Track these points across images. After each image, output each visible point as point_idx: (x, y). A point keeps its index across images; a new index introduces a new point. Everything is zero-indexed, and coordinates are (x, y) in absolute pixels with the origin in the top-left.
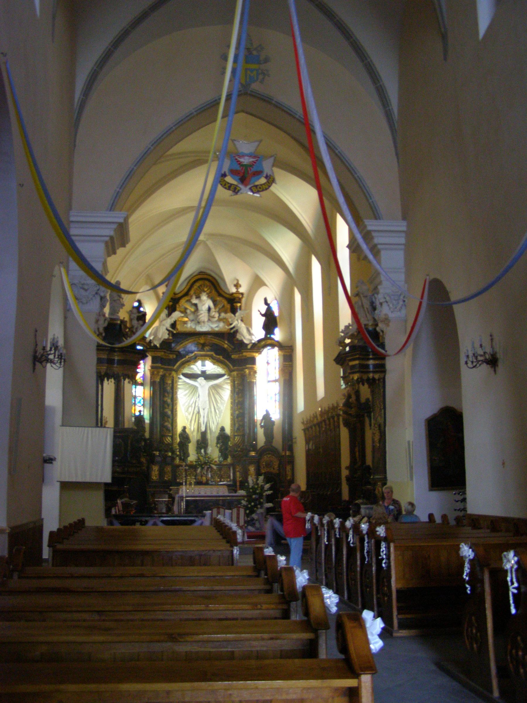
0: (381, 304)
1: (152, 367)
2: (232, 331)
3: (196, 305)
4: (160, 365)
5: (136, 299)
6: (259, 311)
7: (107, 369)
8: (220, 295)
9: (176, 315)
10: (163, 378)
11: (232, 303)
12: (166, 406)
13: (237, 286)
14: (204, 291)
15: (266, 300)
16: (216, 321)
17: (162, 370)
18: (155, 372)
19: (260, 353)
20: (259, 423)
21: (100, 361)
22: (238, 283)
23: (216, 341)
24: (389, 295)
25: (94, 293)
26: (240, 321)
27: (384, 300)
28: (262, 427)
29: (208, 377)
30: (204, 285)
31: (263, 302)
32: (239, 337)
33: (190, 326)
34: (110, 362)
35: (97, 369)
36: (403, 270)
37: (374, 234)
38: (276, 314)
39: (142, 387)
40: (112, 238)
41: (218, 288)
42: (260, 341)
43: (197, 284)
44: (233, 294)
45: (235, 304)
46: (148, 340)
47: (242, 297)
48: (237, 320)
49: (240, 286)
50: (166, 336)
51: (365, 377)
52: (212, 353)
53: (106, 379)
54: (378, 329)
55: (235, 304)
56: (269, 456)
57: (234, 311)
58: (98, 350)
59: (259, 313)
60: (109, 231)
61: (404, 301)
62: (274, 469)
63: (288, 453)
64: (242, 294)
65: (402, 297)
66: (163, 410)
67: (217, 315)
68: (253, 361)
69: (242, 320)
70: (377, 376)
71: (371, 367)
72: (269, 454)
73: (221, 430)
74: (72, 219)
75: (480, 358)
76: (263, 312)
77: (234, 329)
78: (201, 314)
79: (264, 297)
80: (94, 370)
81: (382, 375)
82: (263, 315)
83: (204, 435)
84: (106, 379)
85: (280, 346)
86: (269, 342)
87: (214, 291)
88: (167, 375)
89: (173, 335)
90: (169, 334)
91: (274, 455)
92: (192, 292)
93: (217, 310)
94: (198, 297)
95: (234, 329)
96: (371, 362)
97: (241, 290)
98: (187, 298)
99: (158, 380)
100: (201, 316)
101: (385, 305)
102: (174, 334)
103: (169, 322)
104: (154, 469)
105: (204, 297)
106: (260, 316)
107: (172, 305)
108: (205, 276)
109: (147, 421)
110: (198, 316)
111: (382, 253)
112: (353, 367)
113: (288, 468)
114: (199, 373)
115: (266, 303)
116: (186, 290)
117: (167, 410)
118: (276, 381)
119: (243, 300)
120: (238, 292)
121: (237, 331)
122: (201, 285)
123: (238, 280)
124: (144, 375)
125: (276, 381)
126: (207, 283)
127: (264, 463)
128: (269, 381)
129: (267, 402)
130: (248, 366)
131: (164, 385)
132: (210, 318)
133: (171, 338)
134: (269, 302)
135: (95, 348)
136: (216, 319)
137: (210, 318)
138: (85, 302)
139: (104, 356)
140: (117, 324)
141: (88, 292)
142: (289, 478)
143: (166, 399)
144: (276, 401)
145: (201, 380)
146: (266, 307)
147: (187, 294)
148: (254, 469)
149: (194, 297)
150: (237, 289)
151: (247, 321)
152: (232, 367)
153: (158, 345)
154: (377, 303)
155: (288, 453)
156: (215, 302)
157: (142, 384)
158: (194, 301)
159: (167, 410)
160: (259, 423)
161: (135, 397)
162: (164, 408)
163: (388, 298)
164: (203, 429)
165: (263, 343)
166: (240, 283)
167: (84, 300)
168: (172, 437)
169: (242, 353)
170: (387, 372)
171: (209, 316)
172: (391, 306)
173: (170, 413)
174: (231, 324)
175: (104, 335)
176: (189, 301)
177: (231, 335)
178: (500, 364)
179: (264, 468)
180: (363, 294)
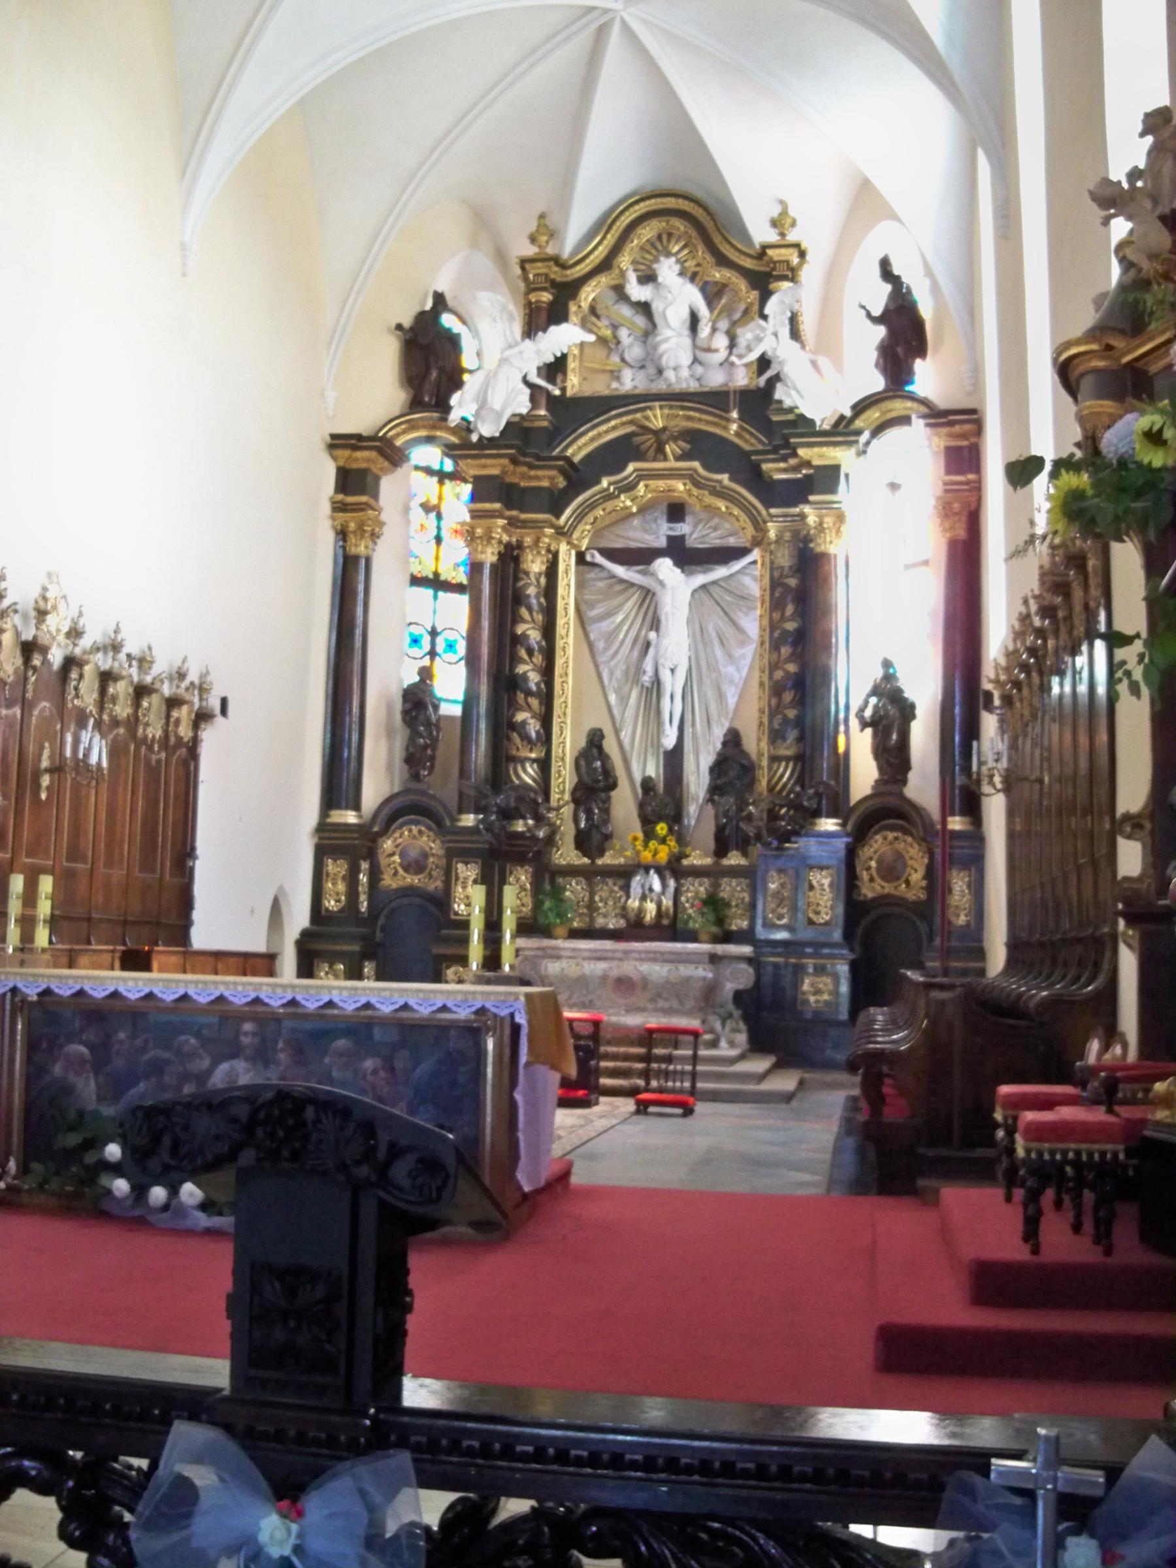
1: (475, 515)
2: (762, 381)
3: (645, 308)
4: (497, 506)
6: (863, 307)
8: (722, 261)
9: (564, 337)
10: (510, 558)
12: (523, 653)
14: (668, 254)
15: (885, 265)
17: (501, 522)
18: (479, 531)
22: (784, 213)
23: (704, 422)
28: (864, 725)
29: (686, 556)
30: (670, 235)
31: (877, 270)
32: (779, 393)
33: (630, 382)
38: (926, 310)
41: (717, 240)
43: (647, 232)
44: (765, 247)
47: (801, 264)
49: (794, 224)
50: (522, 404)
52: (696, 464)
56: (891, 835)
59: (864, 312)
62: (907, 882)
63: (956, 823)
66: (512, 667)
67: (721, 342)
72: (893, 828)
73: (724, 744)
76: (877, 311)
78: (666, 340)
79: (881, 256)
82: (876, 320)
83: (674, 759)
85: (937, 416)
86: (898, 407)
87: (701, 250)
88: (528, 541)
89: (555, 404)
90: (533, 399)
91: (906, 832)
92: (624, 261)
93: (724, 325)
94: (648, 278)
97: (792, 237)
98: (604, 279)
99: (489, 556)
100: (662, 348)
102: (555, 397)
104: (461, 876)
105: (667, 270)
106: (868, 322)
107: (551, 304)
108: (670, 203)
109: (456, 710)
110: (655, 348)
113: (959, 883)
114: (662, 543)
116: (601, 252)
117: (521, 669)
119: (805, 274)
122: (660, 237)
123: (781, 202)
126: (679, 224)
127: (873, 864)
129: (887, 629)
130: (812, 498)
131: (517, 579)
132: (702, 356)
133: (542, 412)
136: (723, 354)
137: (702, 356)
142: (962, 920)
143: (520, 629)
145: (665, 567)
146: (888, 288)
147: (605, 266)
148: (831, 885)
149: (632, 277)
150: (783, 235)
152: (764, 512)
155: (956, 823)
158: (637, 292)
159: (521, 669)
162: (515, 660)
164: (670, 741)
165: (874, 415)
166: (792, 212)
168: (544, 765)
169: (795, 454)
171: (695, 346)
173: (534, 678)
176: (619, 291)
179: (872, 880)
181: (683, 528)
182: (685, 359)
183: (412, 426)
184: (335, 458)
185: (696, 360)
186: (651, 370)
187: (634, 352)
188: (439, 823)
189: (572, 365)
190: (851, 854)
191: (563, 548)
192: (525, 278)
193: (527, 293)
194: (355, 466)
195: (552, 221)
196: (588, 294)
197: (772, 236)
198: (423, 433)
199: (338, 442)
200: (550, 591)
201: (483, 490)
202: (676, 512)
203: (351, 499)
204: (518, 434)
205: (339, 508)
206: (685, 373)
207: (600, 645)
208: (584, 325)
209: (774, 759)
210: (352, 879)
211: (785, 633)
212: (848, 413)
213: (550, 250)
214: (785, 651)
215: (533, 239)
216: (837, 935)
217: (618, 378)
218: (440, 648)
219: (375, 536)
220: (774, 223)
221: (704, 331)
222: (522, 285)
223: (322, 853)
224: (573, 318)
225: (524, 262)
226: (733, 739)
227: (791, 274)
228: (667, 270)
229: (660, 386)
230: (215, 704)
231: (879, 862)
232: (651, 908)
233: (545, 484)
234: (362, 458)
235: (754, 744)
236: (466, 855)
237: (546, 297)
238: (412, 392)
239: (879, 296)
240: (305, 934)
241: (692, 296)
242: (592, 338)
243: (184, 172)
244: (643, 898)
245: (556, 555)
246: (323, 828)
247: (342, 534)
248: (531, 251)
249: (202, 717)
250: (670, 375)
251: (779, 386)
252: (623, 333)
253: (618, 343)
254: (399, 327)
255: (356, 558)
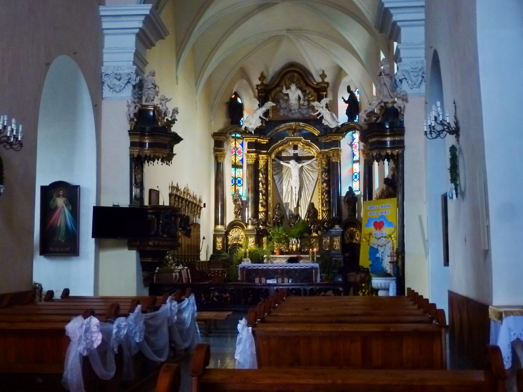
0: (401, 81)
1: (248, 152)
2: (318, 118)
3: (287, 95)
5: (233, 93)
6: (343, 98)
7: (139, 152)
8: (308, 85)
9: (269, 104)
11: (318, 91)
13: (323, 76)
14: (294, 83)
16: (306, 109)
19: (343, 136)
20: (343, 199)
21: (133, 144)
24: (407, 72)
25: (126, 82)
26: (324, 108)
27: (403, 77)
29: (298, 159)
32: (323, 121)
34: (142, 145)
35: (130, 152)
36: (424, 46)
37: (392, 11)
39: (241, 170)
40: (140, 29)
41: (306, 79)
42: (343, 125)
43: (288, 76)
44: (318, 84)
45: (321, 93)
46: (243, 127)
48: (322, 107)
49: (326, 76)
50: (259, 124)
51: (383, 153)
53: (146, 161)
54: (395, 105)
55: (321, 93)
57: (319, 99)
58: (130, 134)
60: (138, 23)
61: (423, 77)
64: (328, 84)
65: (420, 73)
67: (306, 103)
68: (337, 143)
69: (327, 107)
70: (395, 152)
71: (388, 143)
74: (102, 13)
75: (439, 128)
76: (347, 99)
77: (321, 116)
80: (129, 153)
81: (400, 151)
82: (346, 102)
84: (146, 161)
87: (302, 83)
90: (262, 122)
92: (283, 83)
95: (321, 116)
96: (388, 139)
97: (326, 80)
101: (404, 81)
103: (261, 112)
105: (293, 87)
111: (403, 30)
112: (373, 144)
115: (349, 89)
116: (277, 82)
118: (358, 161)
119: (329, 89)
120: (323, 82)
121: (322, 118)
122: (291, 77)
123: (323, 71)
124: (242, 159)
125: (358, 161)
126: (296, 74)
128: (354, 162)
132: (302, 107)
134: (352, 89)
135: (128, 133)
136: (306, 107)
137: (302, 107)
138: (118, 90)
139: (137, 140)
140: (150, 110)
141: (121, 81)
144: (359, 179)
145: (292, 162)
150: (323, 79)
151: (332, 107)
153: (253, 132)
154: (398, 80)
156: (303, 91)
157: (241, 167)
158: (285, 91)
160: (343, 199)
161: (235, 179)
163: (406, 75)
166: (325, 73)
167: (117, 89)
170: (406, 148)
171: (300, 104)
172: (410, 82)
174: (317, 111)
175: (135, 120)
176: (281, 91)
177: (317, 121)
178: (461, 133)
179: (348, 239)
180: (384, 72)
181: (297, 152)
182: (297, 107)
183: (231, 129)
184: (214, 138)
185: (300, 108)
186: (288, 110)
187: (284, 105)
188: (243, 228)
189: (270, 112)
190: (343, 233)
191: (269, 158)
192: (257, 88)
193: (259, 93)
194: (219, 140)
195: (265, 74)
196: (273, 93)
197: (320, 80)
198: (234, 130)
199: (214, 135)
200: (266, 170)
201: (250, 145)
202: (295, 147)
203: (219, 148)
204: (259, 131)
205: (215, 151)
206: (297, 111)
207: (276, 182)
208: (273, 101)
209: (323, 211)
210: (223, 242)
211: (325, 180)
212: (340, 127)
213: (265, 82)
214: (325, 184)
215: (260, 79)
216: (340, 253)
217: (279, 112)
218: (237, 182)
219: (224, 157)
220: (320, 76)
221: (302, 102)
222: (257, 91)
223: (215, 237)
224: (270, 99)
225: (257, 86)
226: (312, 205)
227: (325, 89)
228: (293, 87)
229: (291, 116)
230: (202, 205)
231: (349, 235)
232: (294, 247)
233: (265, 143)
234: (222, 138)
235: (318, 206)
236: (251, 236)
237: (264, 94)
238: (230, 120)
239: (347, 97)
240: (212, 256)
241: (299, 92)
242: (274, 105)
243: (196, 85)
244: (293, 245)
245: (267, 160)
246: (215, 231)
247: (216, 158)
248: (259, 82)
249: (201, 208)
250: (293, 112)
251: (323, 121)
252: (281, 101)
253: (279, 102)
254: (227, 103)
255: (220, 163)
